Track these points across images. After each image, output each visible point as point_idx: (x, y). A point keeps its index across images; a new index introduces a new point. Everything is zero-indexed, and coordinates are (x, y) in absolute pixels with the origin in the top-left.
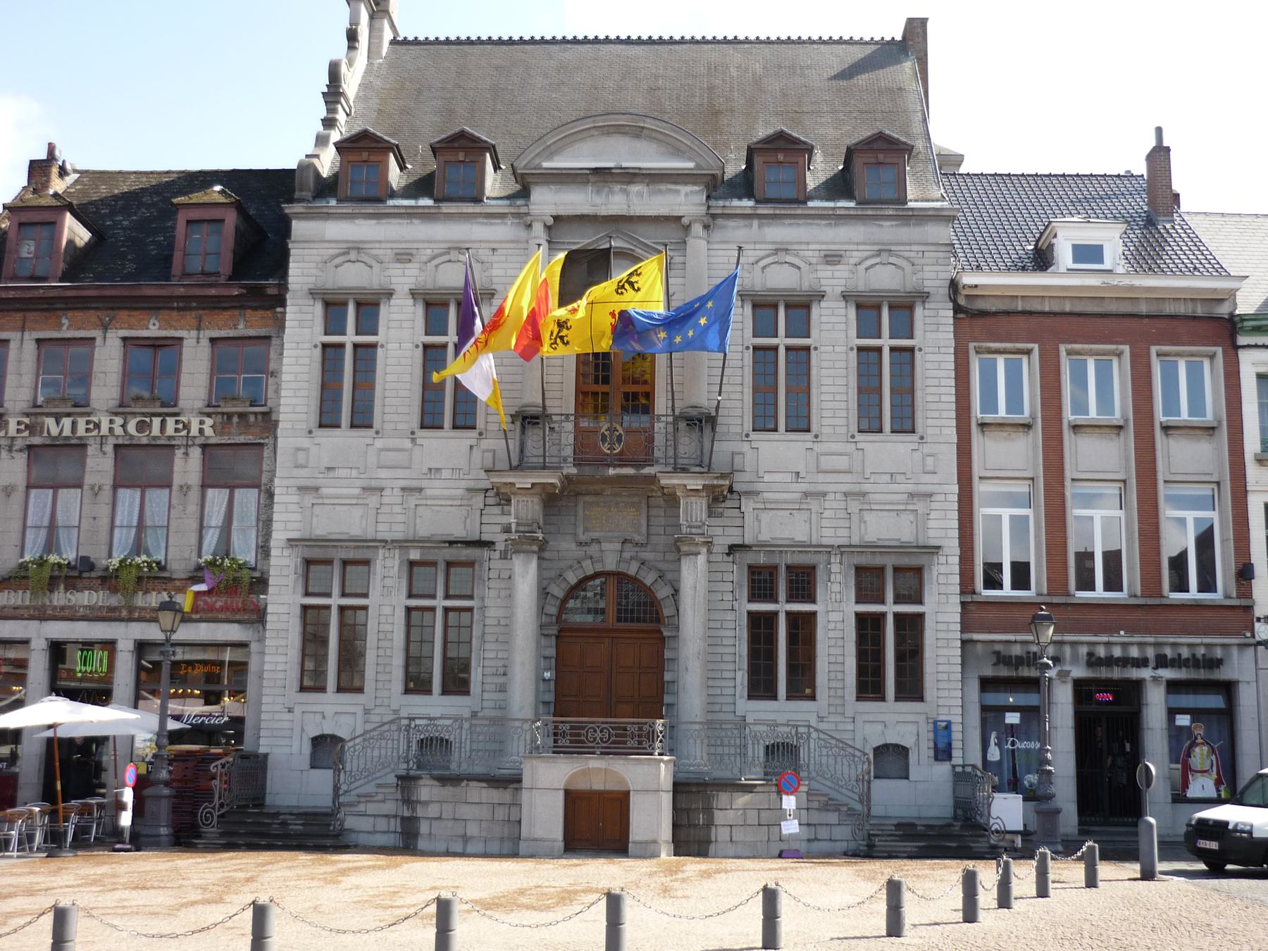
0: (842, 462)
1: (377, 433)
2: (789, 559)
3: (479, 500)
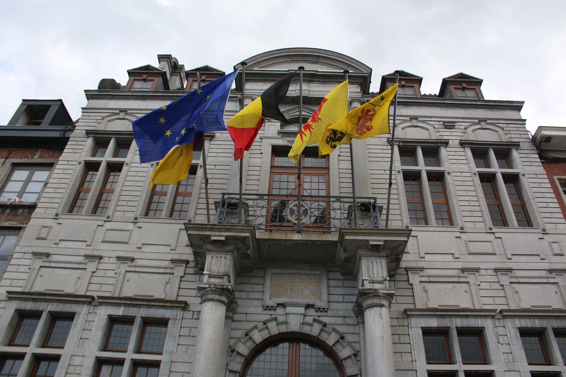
0: (486, 247)
1: (108, 217)
3: (180, 271)
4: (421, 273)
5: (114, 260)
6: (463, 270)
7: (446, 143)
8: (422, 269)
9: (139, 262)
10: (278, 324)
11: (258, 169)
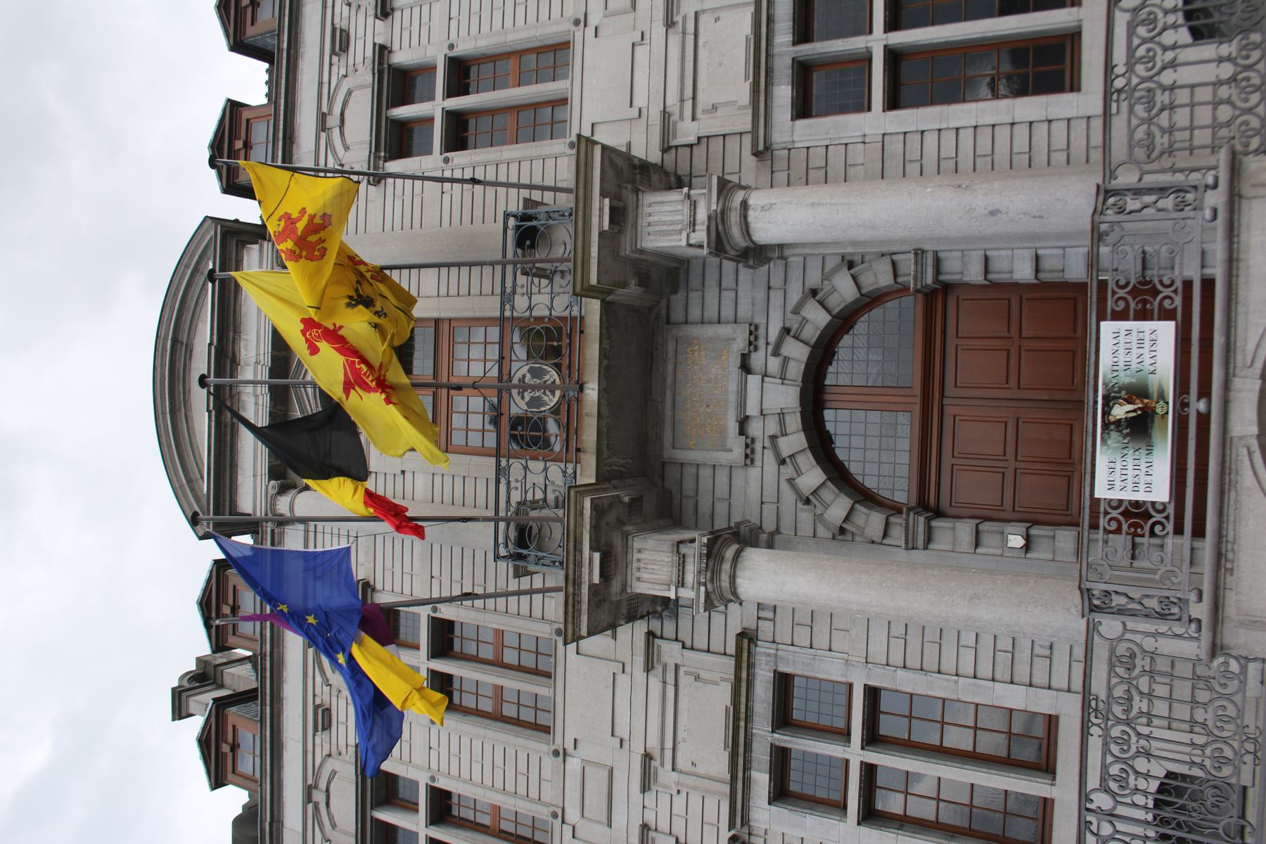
1: (555, 815)
2: (783, 35)
3: (670, 652)
4: (675, 117)
5: (650, 798)
6: (669, 24)
7: (383, 51)
8: (665, 115)
9: (653, 743)
10: (784, 434)
11: (438, 480)
